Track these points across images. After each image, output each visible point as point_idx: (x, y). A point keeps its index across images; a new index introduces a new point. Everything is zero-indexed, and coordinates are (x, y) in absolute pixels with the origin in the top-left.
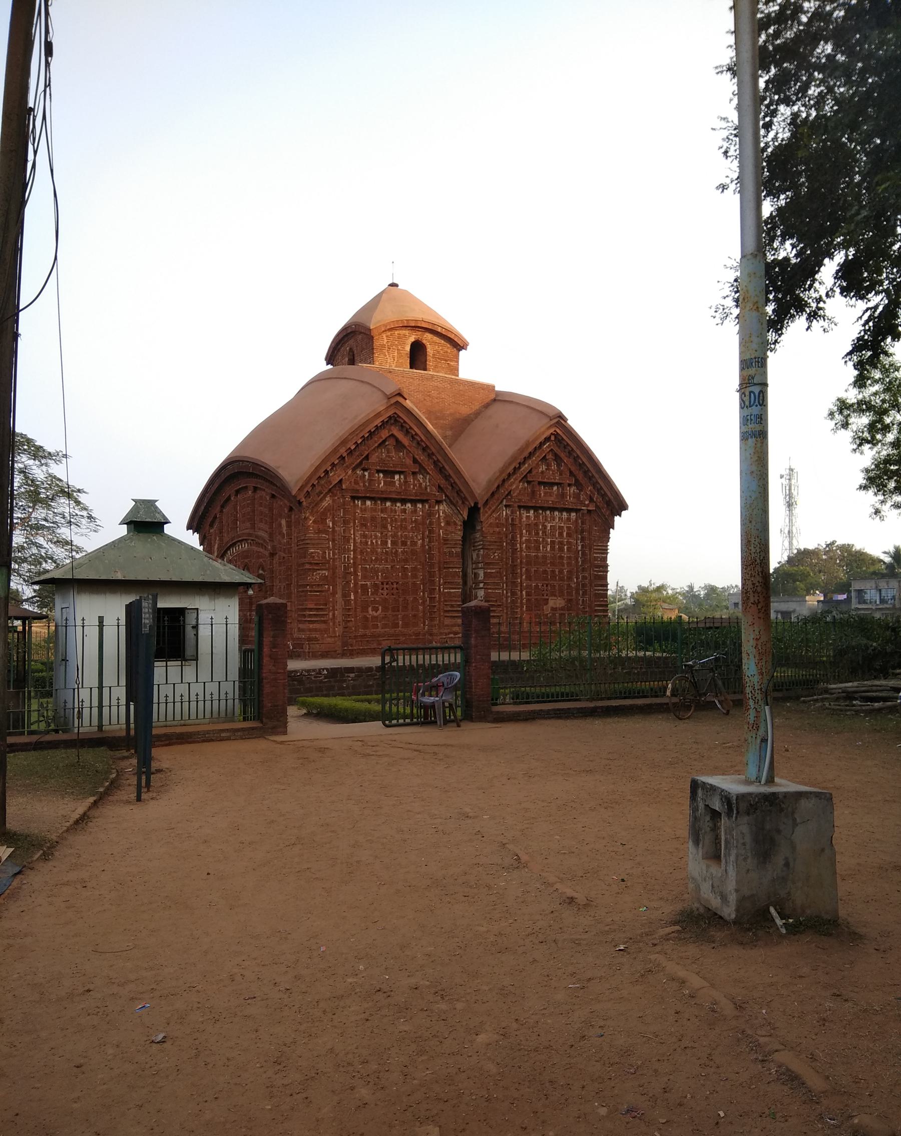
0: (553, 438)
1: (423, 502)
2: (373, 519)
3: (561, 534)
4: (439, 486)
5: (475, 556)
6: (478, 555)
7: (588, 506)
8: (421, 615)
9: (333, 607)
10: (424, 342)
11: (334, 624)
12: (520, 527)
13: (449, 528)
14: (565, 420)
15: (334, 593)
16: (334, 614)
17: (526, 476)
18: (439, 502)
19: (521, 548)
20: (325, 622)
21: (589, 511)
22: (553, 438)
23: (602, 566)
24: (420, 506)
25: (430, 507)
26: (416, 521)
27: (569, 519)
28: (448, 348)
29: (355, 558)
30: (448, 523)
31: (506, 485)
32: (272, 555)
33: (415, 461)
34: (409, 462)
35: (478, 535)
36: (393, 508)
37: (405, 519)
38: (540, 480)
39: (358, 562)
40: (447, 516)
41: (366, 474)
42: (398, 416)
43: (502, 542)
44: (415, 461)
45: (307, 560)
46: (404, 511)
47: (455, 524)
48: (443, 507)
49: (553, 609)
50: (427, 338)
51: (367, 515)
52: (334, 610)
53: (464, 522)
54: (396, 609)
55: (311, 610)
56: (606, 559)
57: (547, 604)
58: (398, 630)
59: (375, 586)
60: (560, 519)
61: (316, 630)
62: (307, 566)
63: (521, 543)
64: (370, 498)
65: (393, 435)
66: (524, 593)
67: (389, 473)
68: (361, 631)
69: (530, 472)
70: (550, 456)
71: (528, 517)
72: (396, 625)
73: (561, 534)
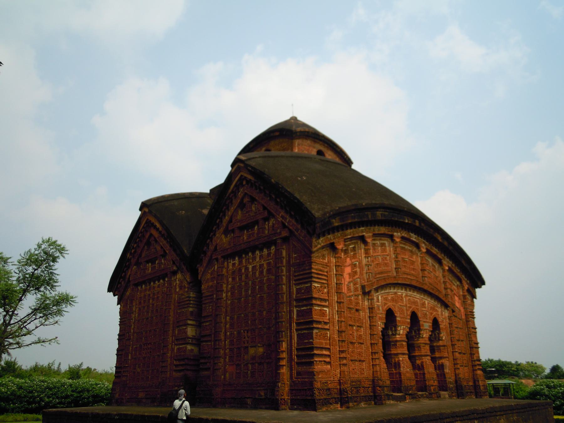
0: (244, 183)
2: (145, 296)
3: (261, 272)
18: (174, 273)
19: (227, 296)
21: (285, 240)
22: (244, 183)
27: (269, 254)
30: (181, 288)
34: (159, 248)
38: (239, 224)
46: (159, 286)
47: (185, 287)
48: (179, 276)
49: (253, 358)
51: (142, 295)
57: (247, 353)
60: (261, 257)
64: (144, 282)
67: (153, 261)
69: (230, 221)
70: (246, 200)
71: (234, 264)
73: (261, 272)
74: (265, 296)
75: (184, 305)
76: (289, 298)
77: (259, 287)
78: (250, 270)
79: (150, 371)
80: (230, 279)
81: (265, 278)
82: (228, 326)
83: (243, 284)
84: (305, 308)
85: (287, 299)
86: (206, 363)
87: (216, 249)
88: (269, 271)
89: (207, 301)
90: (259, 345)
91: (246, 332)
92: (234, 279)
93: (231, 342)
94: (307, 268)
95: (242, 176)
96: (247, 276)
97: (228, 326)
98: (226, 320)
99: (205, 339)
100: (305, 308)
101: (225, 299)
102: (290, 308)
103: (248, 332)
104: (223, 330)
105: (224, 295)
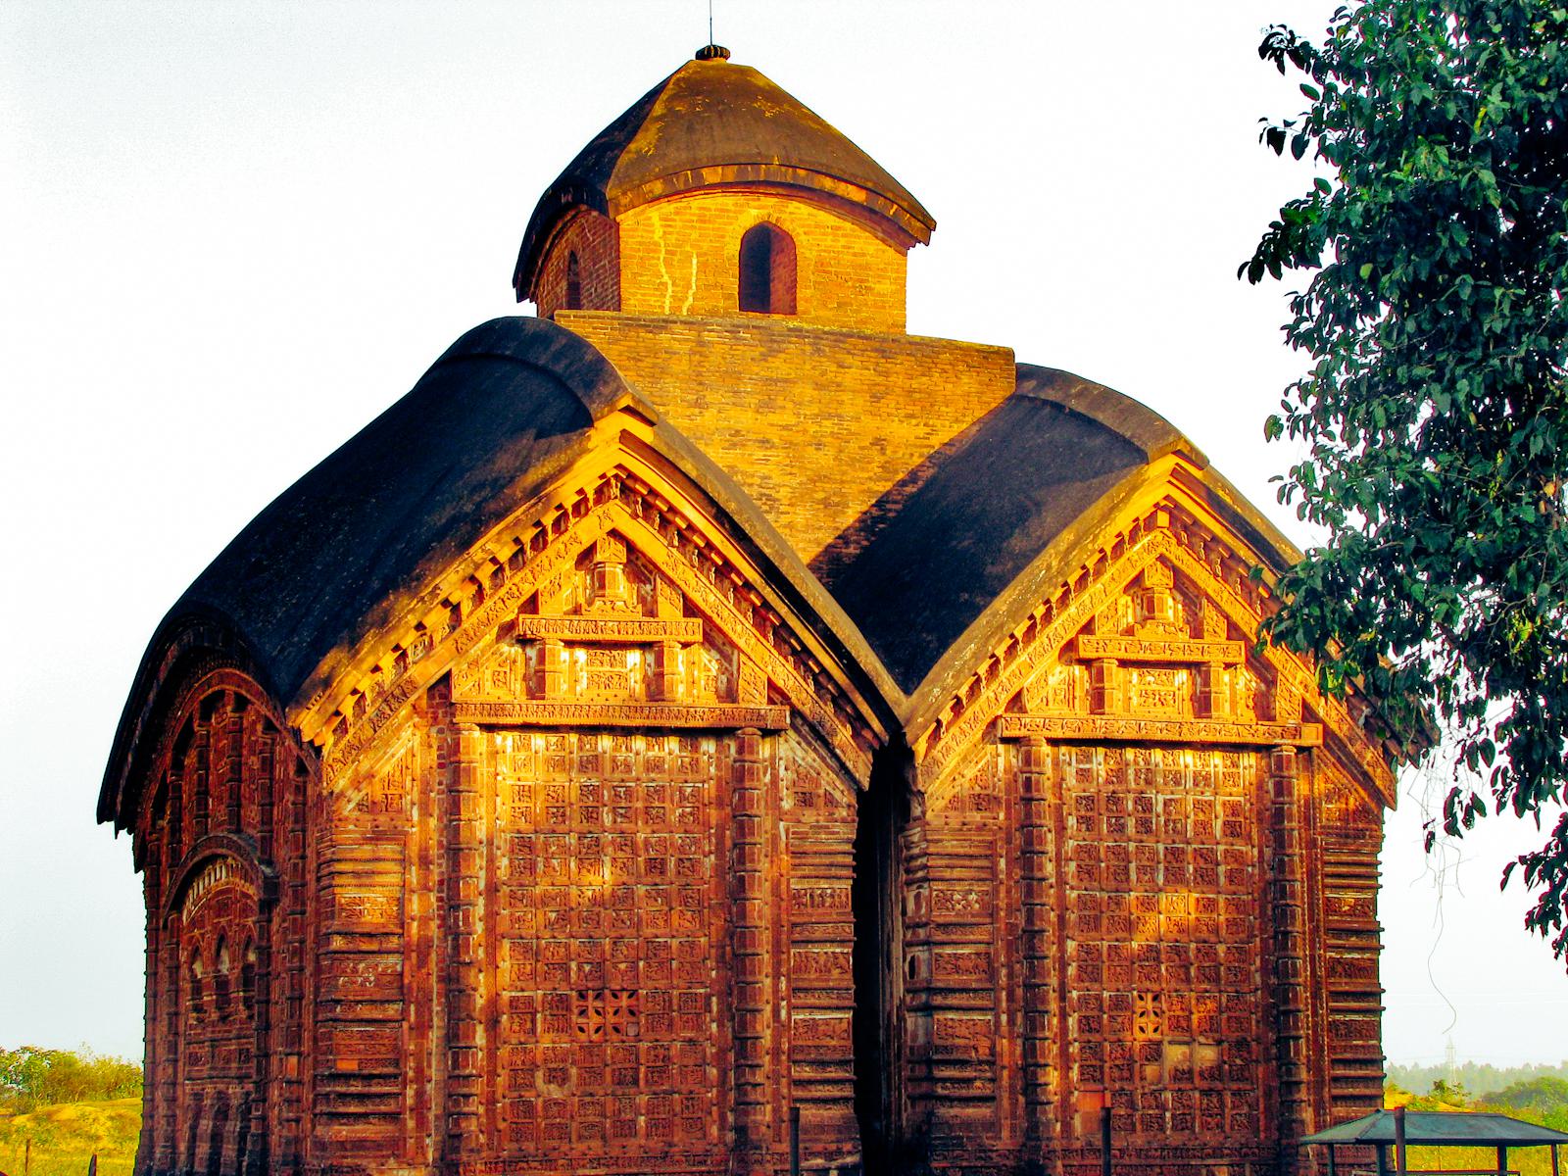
1: (718, 733)
4: (771, 685)
5: (911, 906)
6: (918, 896)
7: (1297, 732)
8: (712, 1094)
9: (419, 1071)
10: (787, 226)
11: (421, 1122)
12: (1059, 808)
13: (809, 817)
14: (1201, 462)
15: (422, 1028)
16: (420, 1094)
17: (1071, 646)
20: (393, 1117)
22: (1163, 519)
23: (1357, 933)
24: (708, 746)
25: (741, 750)
26: (696, 794)
28: (867, 245)
29: (491, 916)
30: (806, 800)
31: (1004, 675)
32: (267, 906)
33: (690, 609)
34: (669, 608)
35: (915, 834)
36: (621, 755)
37: (660, 791)
38: (1123, 655)
39: (503, 926)
40: (801, 777)
41: (532, 652)
42: (631, 475)
43: (992, 857)
44: (690, 609)
45: (336, 924)
47: (830, 800)
49: (1183, 1075)
50: (798, 218)
52: (421, 1077)
53: (860, 793)
54: (627, 1079)
55: (347, 1077)
56: (1369, 908)
58: (634, 1145)
59: (563, 1002)
61: (360, 1145)
62: (338, 943)
63: (1059, 860)
65: (614, 534)
66: (1072, 1021)
68: (508, 1150)
69: (1088, 628)
71: (1084, 775)
72: (627, 1129)
74: (1221, 899)
75: (831, 865)
76: (1311, 920)
77: (1195, 870)
78: (1160, 808)
79: (642, 1100)
80: (1072, 821)
81: (1221, 848)
82: (1072, 970)
83: (1132, 846)
84: (1357, 956)
85: (1304, 924)
86: (969, 1081)
87: (1016, 702)
88: (1232, 829)
89: (956, 873)
90: (1202, 1039)
91: (1150, 996)
92: (1087, 822)
93: (1086, 1025)
94: (1366, 850)
95: (1167, 498)
96: (1145, 826)
97: (1072, 970)
98: (1062, 949)
99: (951, 1001)
100: (1357, 956)
101: (1053, 880)
102: (1313, 948)
103: (1155, 998)
104: (1054, 981)
105: (1050, 868)
